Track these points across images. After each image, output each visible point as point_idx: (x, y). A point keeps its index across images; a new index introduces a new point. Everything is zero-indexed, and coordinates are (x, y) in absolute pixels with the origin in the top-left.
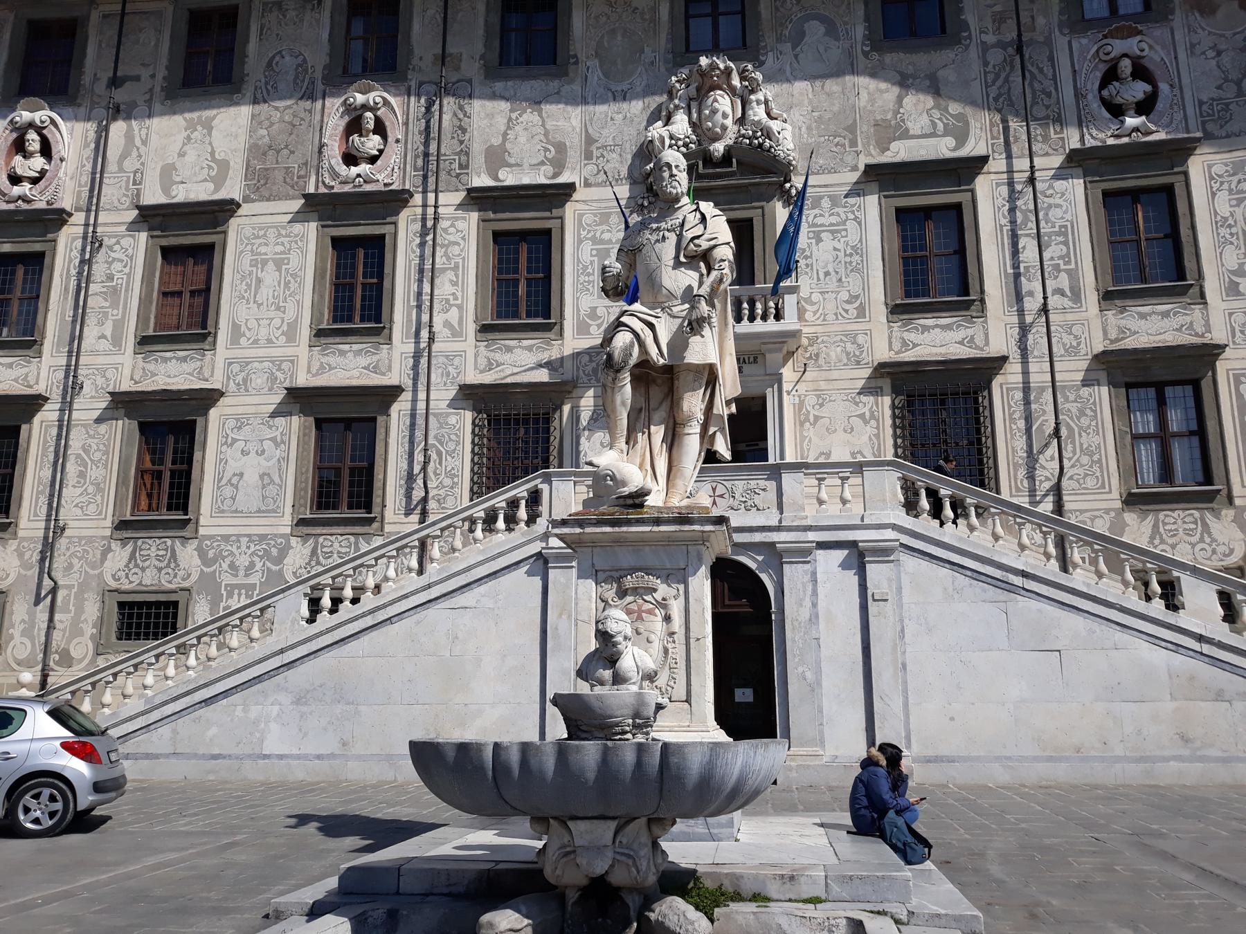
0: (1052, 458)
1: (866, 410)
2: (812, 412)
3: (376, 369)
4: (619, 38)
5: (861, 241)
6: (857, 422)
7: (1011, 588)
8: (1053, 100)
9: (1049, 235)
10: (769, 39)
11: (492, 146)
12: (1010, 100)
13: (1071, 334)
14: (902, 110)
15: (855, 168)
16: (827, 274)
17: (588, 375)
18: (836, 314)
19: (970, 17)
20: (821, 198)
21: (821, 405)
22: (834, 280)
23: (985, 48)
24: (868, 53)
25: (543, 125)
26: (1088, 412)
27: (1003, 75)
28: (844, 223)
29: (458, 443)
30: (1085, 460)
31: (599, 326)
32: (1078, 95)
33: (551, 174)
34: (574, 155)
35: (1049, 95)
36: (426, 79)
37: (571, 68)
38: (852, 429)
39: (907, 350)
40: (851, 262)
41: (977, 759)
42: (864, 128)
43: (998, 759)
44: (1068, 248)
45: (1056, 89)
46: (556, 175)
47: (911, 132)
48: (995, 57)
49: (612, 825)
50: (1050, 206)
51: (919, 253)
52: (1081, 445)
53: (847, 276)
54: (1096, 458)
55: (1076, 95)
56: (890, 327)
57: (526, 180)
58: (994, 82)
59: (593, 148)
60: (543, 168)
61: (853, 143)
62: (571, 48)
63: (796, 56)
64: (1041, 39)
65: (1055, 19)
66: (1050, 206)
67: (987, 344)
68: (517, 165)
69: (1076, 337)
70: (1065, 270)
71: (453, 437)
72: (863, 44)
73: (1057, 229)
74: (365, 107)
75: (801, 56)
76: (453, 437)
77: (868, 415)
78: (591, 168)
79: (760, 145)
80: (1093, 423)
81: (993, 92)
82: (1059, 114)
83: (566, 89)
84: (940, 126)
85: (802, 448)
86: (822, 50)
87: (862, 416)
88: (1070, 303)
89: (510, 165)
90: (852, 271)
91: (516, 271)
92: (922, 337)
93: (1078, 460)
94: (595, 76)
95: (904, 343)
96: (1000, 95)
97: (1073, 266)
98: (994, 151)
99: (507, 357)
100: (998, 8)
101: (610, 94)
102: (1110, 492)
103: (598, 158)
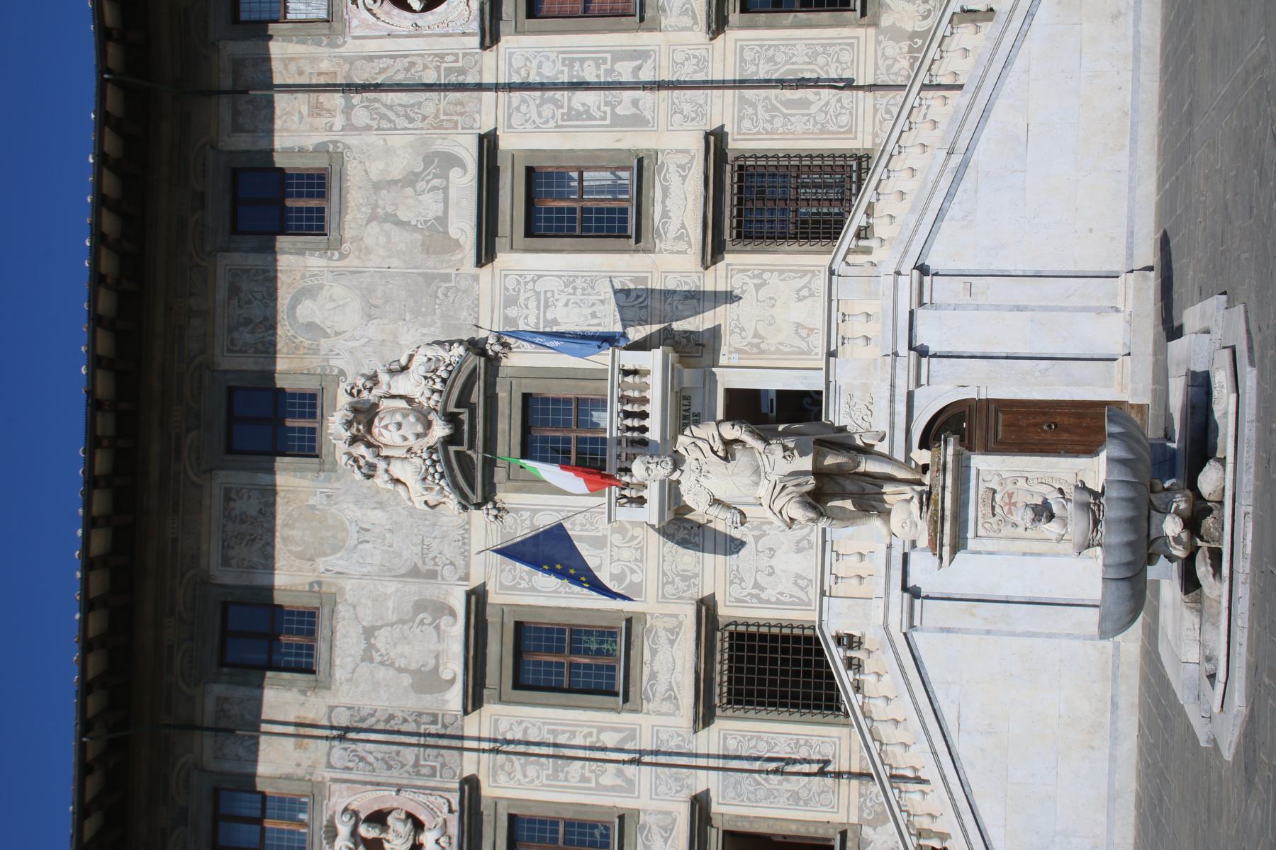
0: (816, 94)
1: (751, 282)
2: (749, 339)
3: (668, 830)
4: (294, 533)
5: (559, 277)
6: (763, 293)
7: (965, 164)
8: (419, 61)
9: (570, 75)
10: (314, 363)
11: (412, 685)
12: (413, 105)
13: (683, 64)
14: (414, 223)
15: (476, 278)
16: (594, 315)
17: (689, 586)
18: (641, 308)
19: (310, 141)
20: (506, 318)
21: (742, 329)
22: (602, 307)
23: (349, 127)
24: (341, 254)
25: (392, 625)
26: (770, 53)
27: (384, 110)
28: (537, 294)
29: (759, 738)
30: (821, 60)
31: (633, 571)
32: (417, 32)
33: (451, 619)
34: (431, 591)
35: (413, 64)
36: (324, 760)
37: (324, 588)
38: (771, 298)
39: (688, 235)
40: (583, 289)
41: (1130, 209)
42: (433, 265)
43: (1131, 190)
44: (588, 59)
45: (406, 56)
46: (452, 613)
47: (440, 214)
48: (361, 116)
49: (1153, 512)
50: (539, 74)
51: (578, 215)
52: (805, 63)
53: (598, 293)
54: (820, 49)
55: (416, 36)
56: (660, 252)
57: (457, 648)
58: (390, 121)
59: (423, 569)
60: (443, 627)
61: (446, 278)
62: (300, 588)
63: (337, 334)
64: (347, 66)
65: (322, 51)
66: (539, 74)
67: (687, 151)
68: (437, 657)
69: (687, 59)
70: (612, 65)
71: (753, 743)
72: (330, 259)
73: (566, 69)
74: (354, 833)
75: (337, 328)
76: (753, 743)
77: (757, 281)
78: (447, 571)
79: (444, 381)
80: (783, 49)
81: (402, 122)
82: (436, 55)
83: (349, 597)
84: (436, 182)
85: (787, 353)
86: (333, 305)
87: (758, 287)
88: (650, 61)
89: (436, 668)
90: (593, 288)
91: (560, 665)
92: (674, 218)
93: (822, 68)
94: (336, 562)
95: (679, 238)
96: (407, 116)
97: (609, 56)
98: (472, 128)
99: (663, 678)
100: (305, 110)
101: (361, 546)
102: (858, 38)
103: (436, 564)
